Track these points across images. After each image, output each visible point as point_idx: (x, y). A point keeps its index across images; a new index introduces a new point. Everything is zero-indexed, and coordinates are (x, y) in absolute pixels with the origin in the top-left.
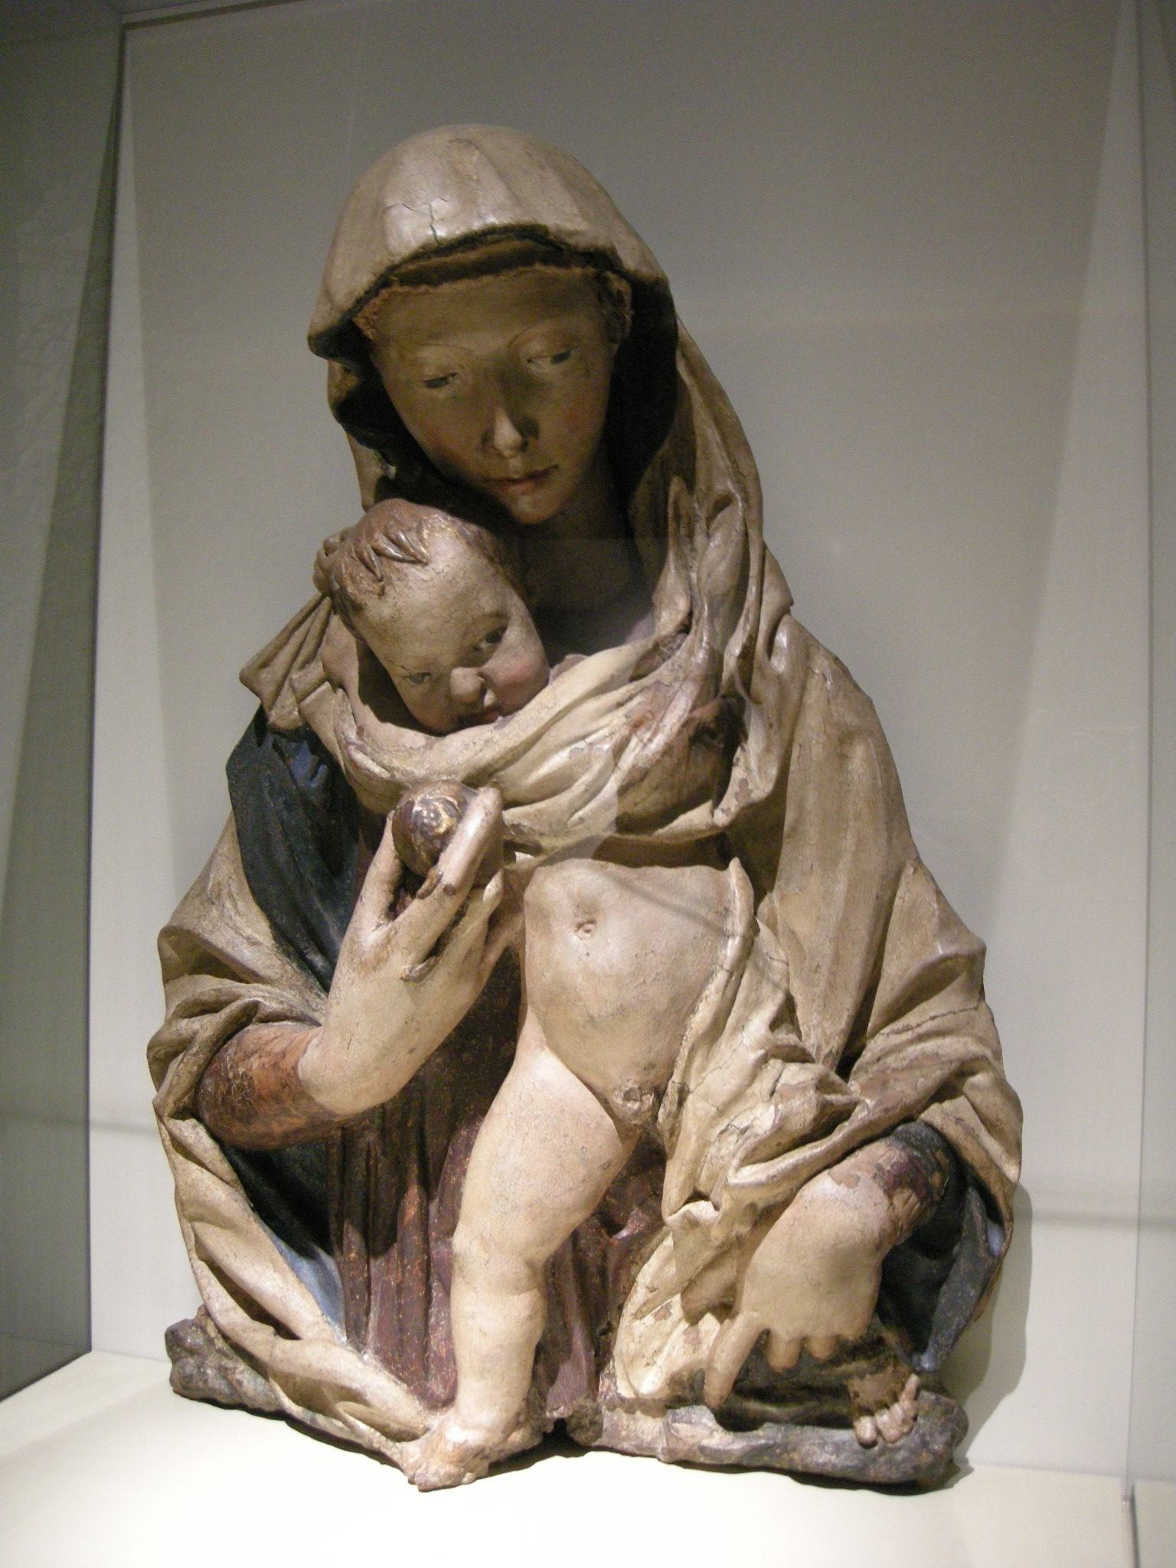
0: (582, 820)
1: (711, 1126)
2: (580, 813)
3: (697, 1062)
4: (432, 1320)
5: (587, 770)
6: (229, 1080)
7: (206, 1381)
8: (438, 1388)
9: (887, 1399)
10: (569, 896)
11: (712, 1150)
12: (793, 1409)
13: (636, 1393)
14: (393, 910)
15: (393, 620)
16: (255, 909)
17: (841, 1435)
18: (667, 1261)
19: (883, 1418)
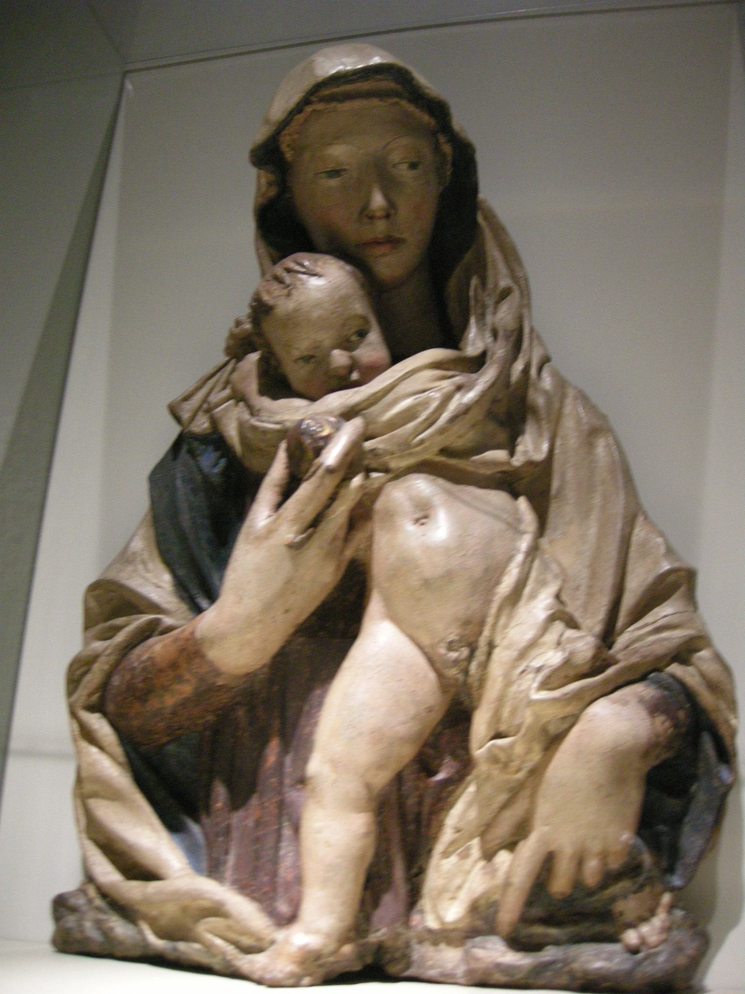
0: (422, 442)
1: (514, 667)
3: (503, 621)
8: (283, 908)
9: (646, 914)
11: (514, 688)
12: (569, 930)
13: (442, 923)
15: (296, 310)
18: (470, 805)
19: (645, 929)
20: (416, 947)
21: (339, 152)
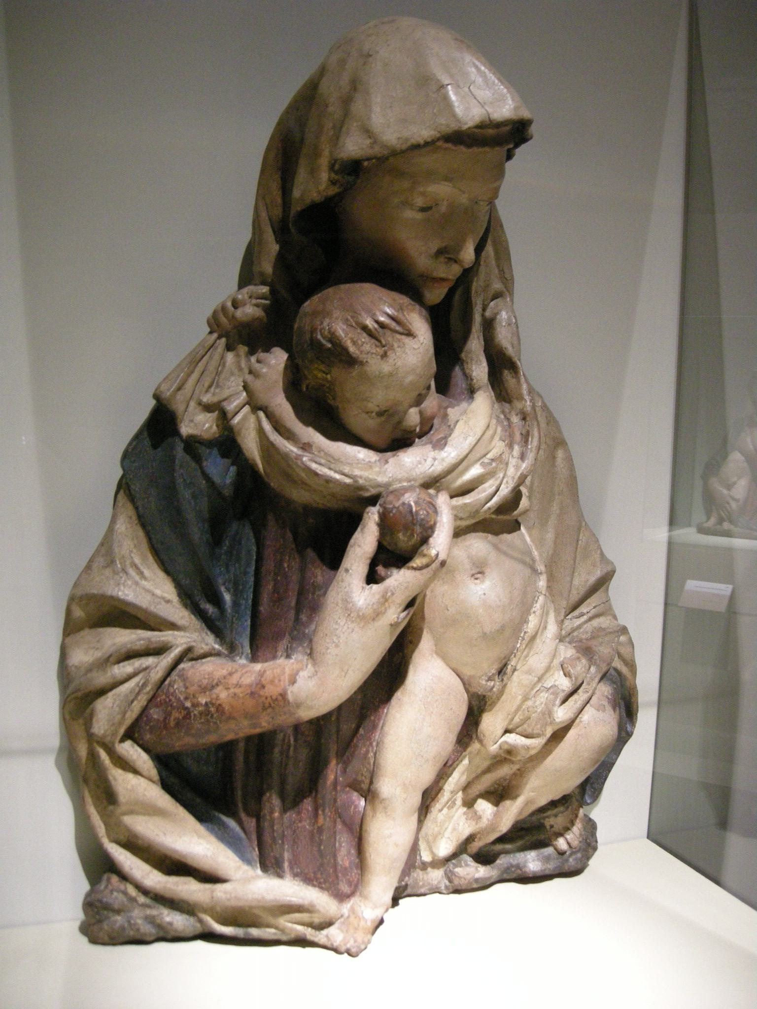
1: (532, 689)
2: (489, 505)
4: (337, 844)
6: (187, 708)
7: (138, 930)
9: (569, 825)
10: (469, 557)
11: (529, 703)
12: (520, 843)
14: (372, 578)
15: (391, 375)
16: (161, 575)
17: (549, 850)
19: (569, 836)
21: (441, 190)
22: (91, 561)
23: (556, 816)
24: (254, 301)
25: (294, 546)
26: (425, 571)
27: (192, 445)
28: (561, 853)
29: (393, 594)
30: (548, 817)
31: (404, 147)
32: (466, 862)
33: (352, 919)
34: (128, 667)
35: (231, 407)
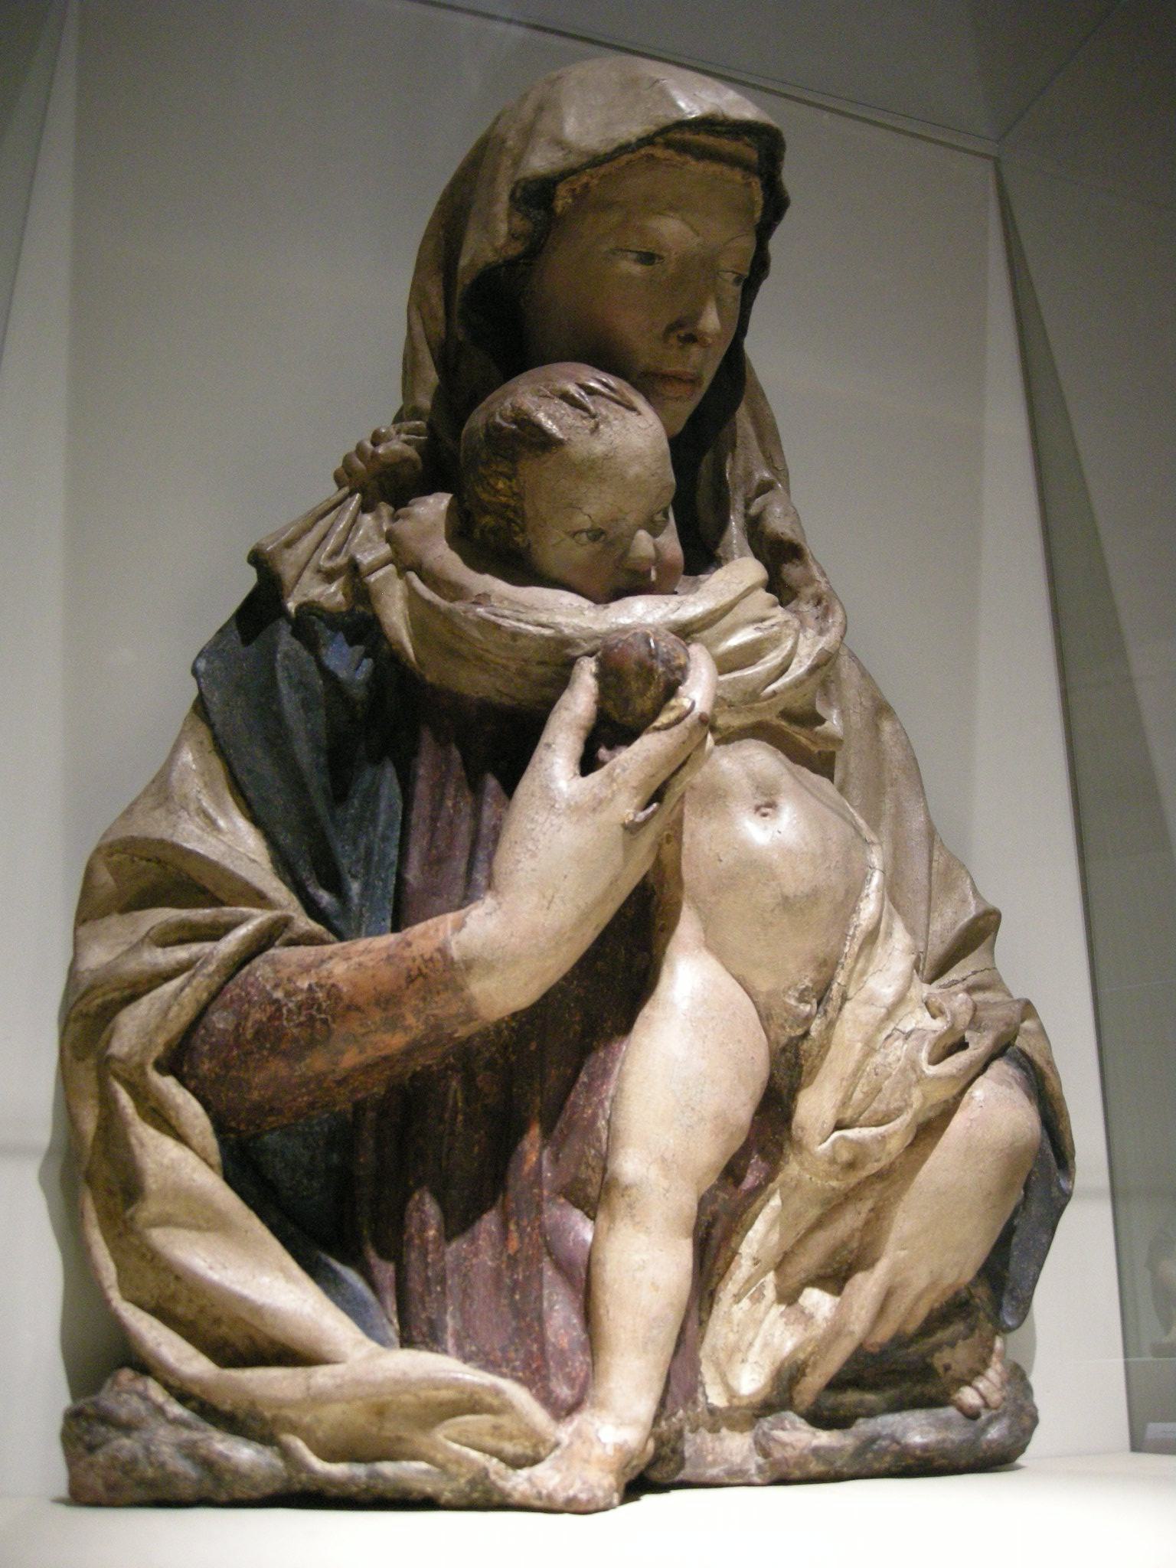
0: (774, 693)
1: (879, 1029)
3: (859, 966)
4: (545, 1304)
5: (776, 647)
6: (277, 1001)
8: (564, 1392)
9: (978, 1366)
11: (877, 1059)
12: (891, 1393)
13: (731, 1393)
14: (588, 764)
15: (606, 457)
17: (951, 1411)
19: (981, 1384)
20: (688, 1435)
22: (135, 803)
23: (952, 1345)
24: (403, 436)
25: (463, 774)
26: (675, 730)
27: (308, 624)
28: (972, 1415)
29: (624, 770)
30: (939, 1347)
31: (610, 148)
32: (792, 1423)
33: (578, 1444)
34: (182, 953)
35: (365, 559)
